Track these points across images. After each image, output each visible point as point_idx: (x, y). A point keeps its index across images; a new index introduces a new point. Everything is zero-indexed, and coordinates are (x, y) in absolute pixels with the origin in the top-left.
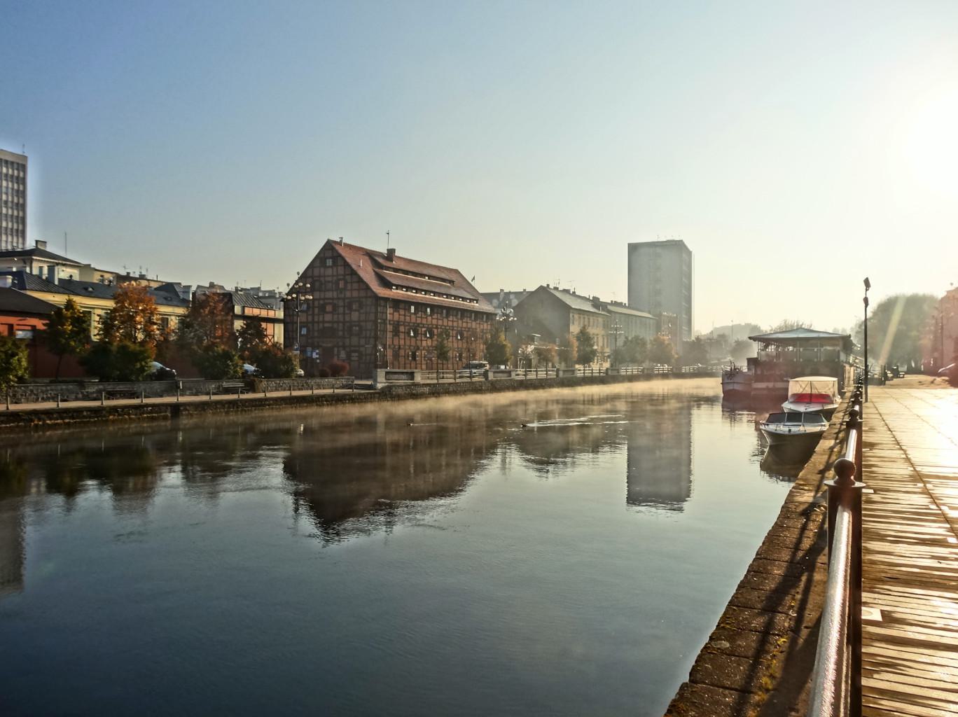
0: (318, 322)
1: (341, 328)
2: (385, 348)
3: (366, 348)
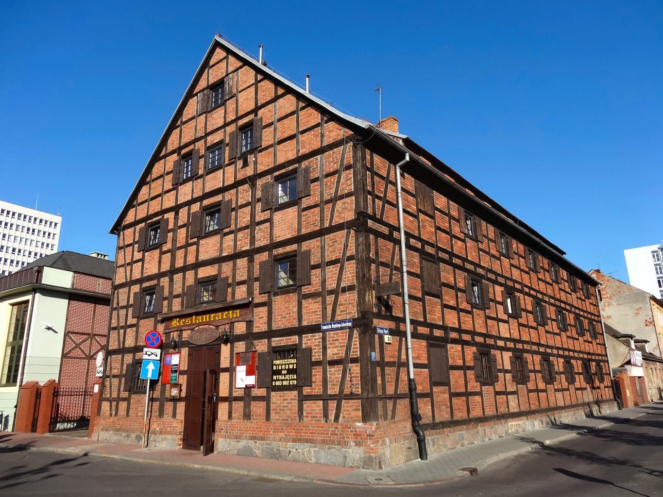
0: (184, 269)
1: (242, 275)
3: (324, 331)
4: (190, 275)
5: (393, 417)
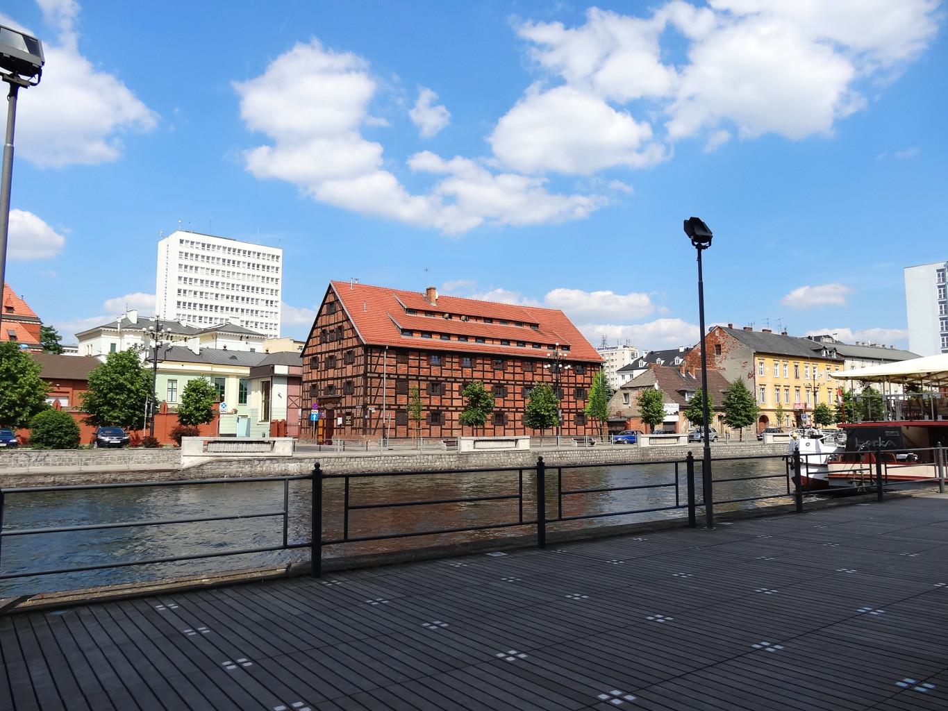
0: (324, 380)
2: (379, 408)
4: (326, 382)
5: (374, 434)
